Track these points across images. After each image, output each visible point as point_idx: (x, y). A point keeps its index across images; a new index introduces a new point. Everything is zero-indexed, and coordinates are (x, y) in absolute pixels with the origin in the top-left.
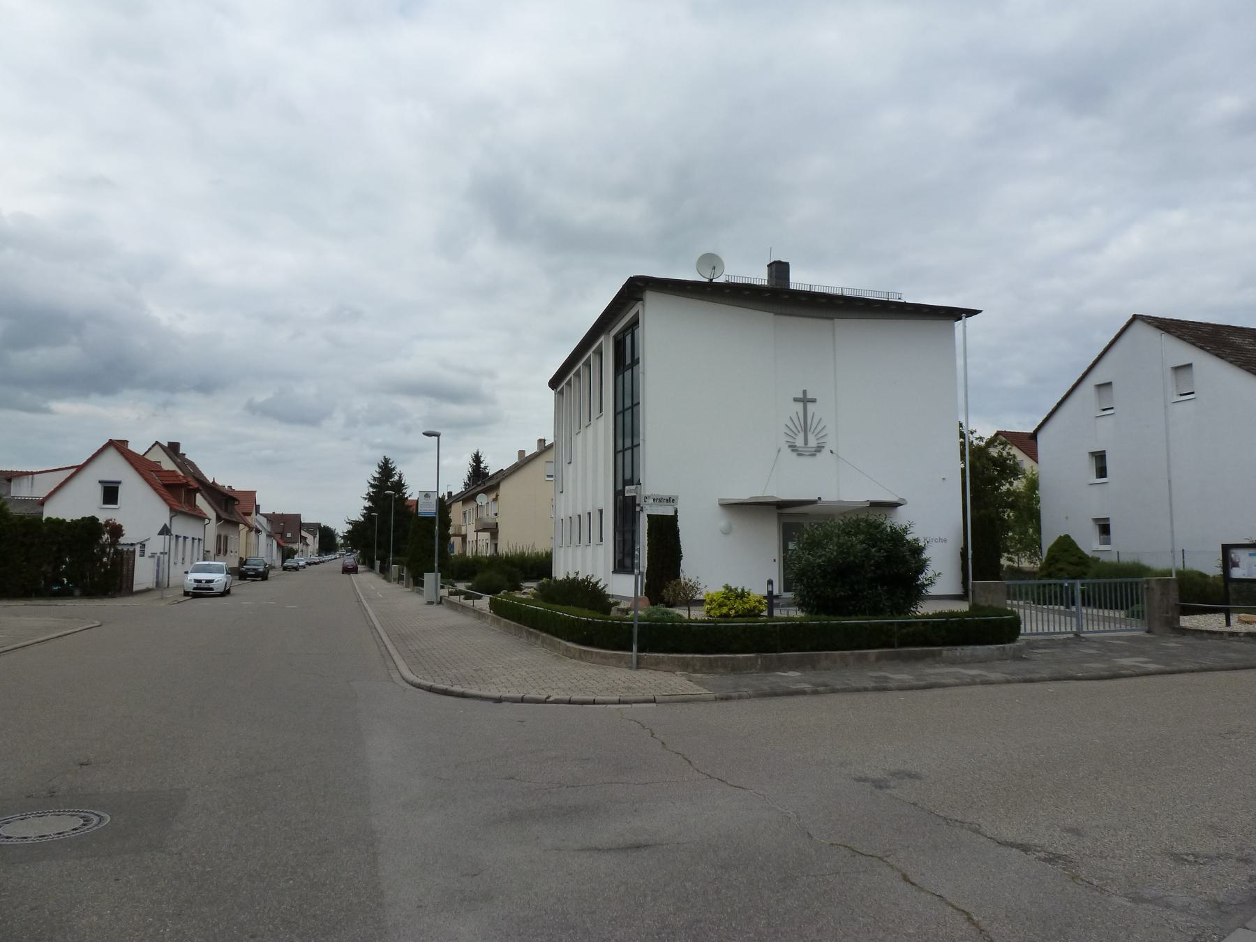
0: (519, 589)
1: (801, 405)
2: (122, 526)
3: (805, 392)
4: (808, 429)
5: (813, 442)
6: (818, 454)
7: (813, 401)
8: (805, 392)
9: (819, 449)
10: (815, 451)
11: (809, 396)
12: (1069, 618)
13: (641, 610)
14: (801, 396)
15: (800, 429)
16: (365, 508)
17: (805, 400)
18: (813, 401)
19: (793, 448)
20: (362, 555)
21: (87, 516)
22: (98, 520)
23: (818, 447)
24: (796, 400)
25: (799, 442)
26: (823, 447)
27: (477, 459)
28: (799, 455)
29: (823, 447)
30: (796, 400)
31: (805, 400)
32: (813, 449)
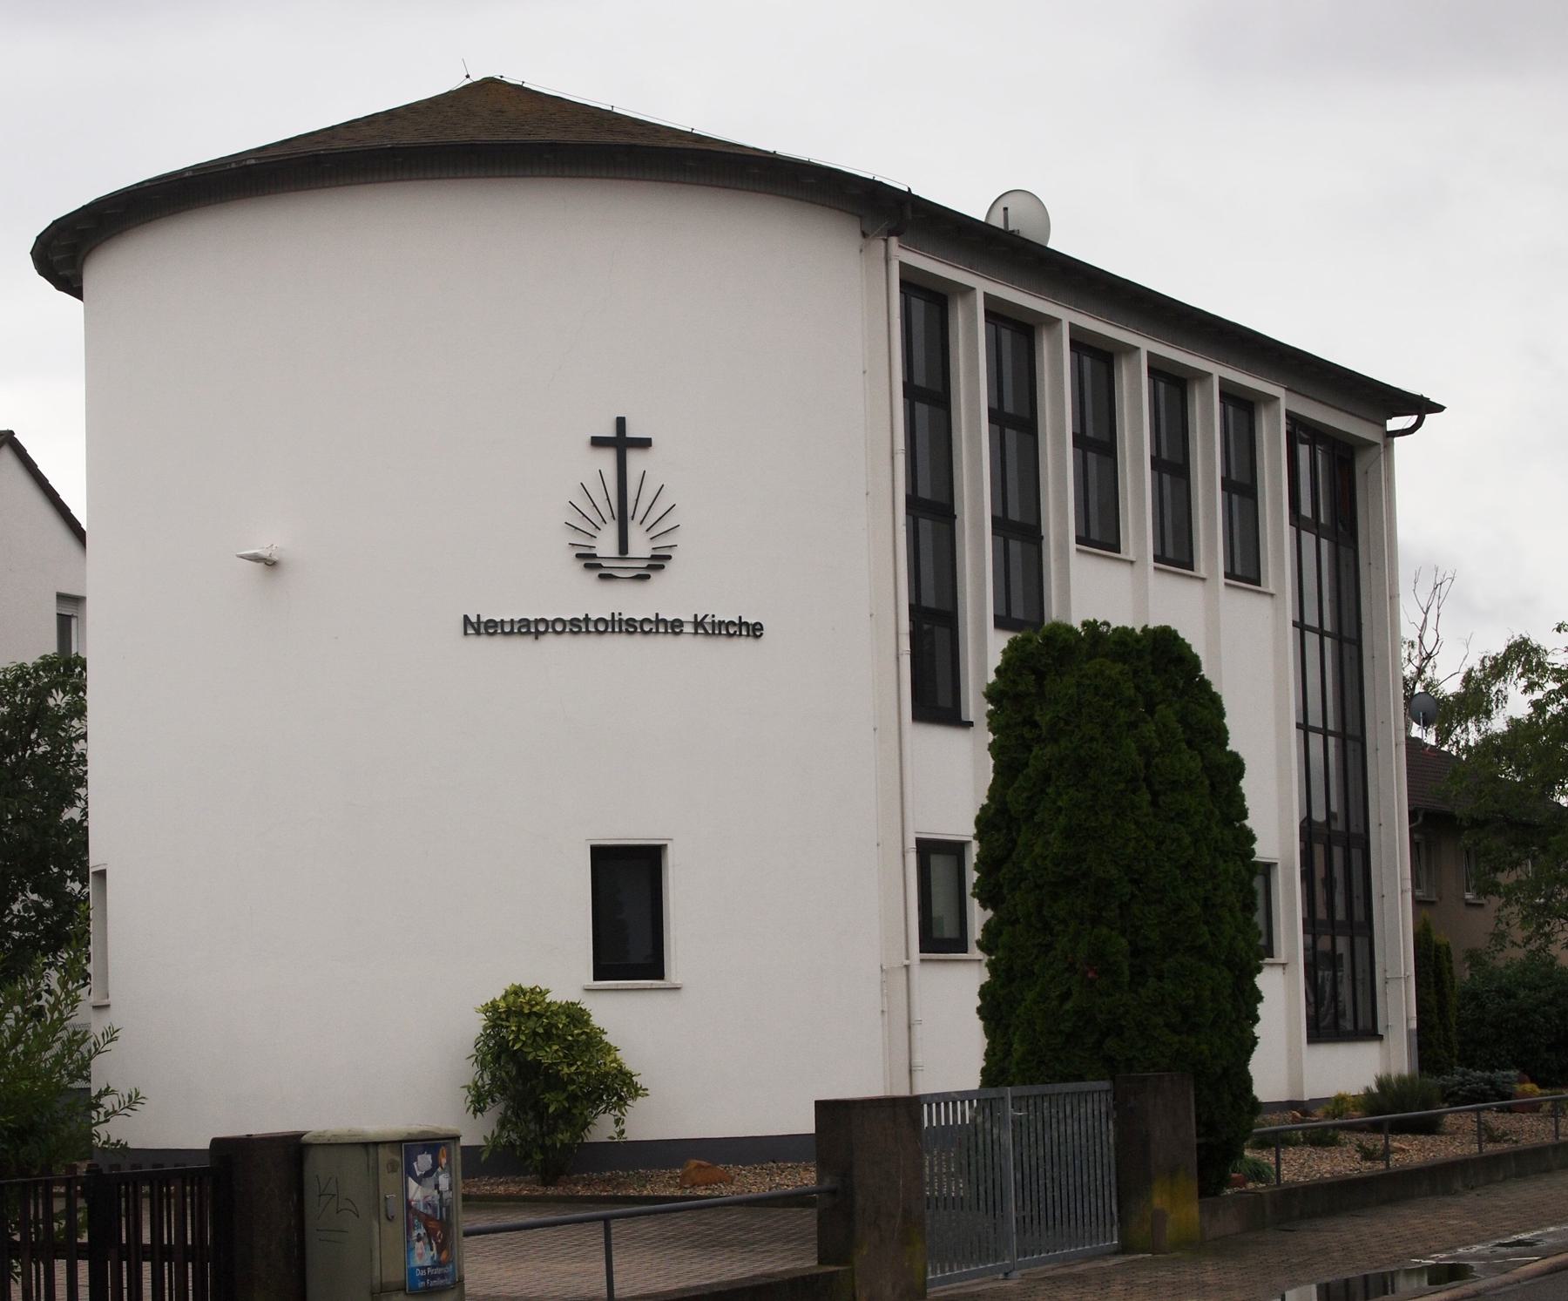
0: (1341, 955)
1: (607, 458)
2: (978, 1009)
3: (621, 423)
4: (630, 513)
5: (640, 546)
6: (654, 575)
7: (645, 443)
8: (621, 423)
9: (658, 562)
10: (649, 567)
11: (632, 432)
12: (1353, 829)
13: (60, 1185)
14: (609, 431)
15: (606, 514)
16: (1133, 629)
17: (621, 443)
18: (645, 443)
19: (589, 561)
20: (93, 1109)
21: (39, 468)
22: (984, 992)
23: (653, 557)
24: (597, 442)
25: (606, 545)
26: (669, 557)
27: (1438, 408)
28: (602, 577)
29: (669, 557)
30: (597, 442)
31: (621, 443)
32: (645, 564)
